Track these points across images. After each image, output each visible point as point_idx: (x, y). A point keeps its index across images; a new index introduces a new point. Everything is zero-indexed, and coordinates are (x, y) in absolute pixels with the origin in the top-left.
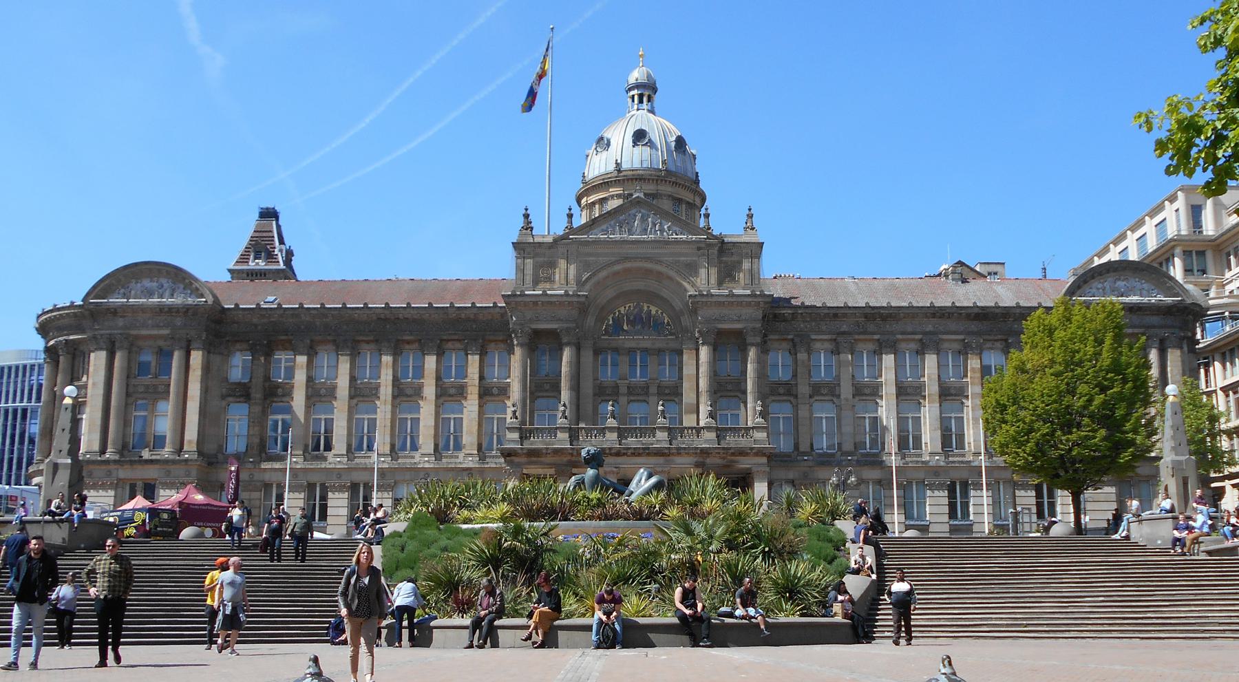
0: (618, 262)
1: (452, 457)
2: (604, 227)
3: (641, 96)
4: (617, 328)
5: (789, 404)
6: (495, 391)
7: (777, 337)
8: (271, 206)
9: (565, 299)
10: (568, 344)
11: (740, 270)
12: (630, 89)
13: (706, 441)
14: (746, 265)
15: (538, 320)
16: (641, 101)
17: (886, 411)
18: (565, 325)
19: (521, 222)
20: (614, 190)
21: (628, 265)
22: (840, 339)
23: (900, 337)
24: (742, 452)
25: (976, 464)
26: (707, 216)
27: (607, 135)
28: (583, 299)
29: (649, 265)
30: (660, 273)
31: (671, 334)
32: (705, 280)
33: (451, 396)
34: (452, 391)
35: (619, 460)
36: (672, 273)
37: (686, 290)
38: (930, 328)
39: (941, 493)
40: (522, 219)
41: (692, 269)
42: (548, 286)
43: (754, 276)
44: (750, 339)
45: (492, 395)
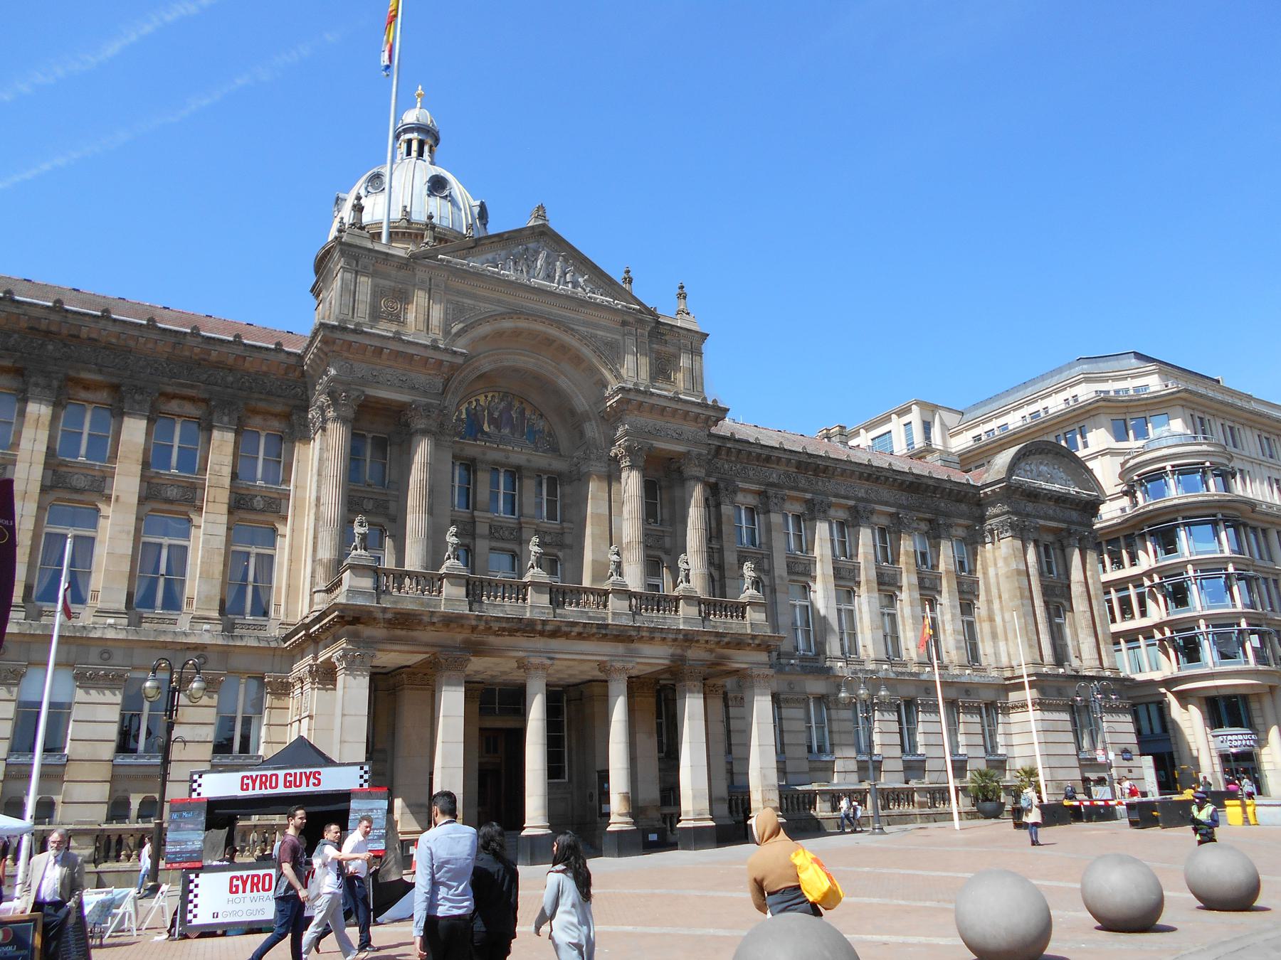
1: (162, 620)
2: (490, 256)
6: (258, 503)
9: (430, 353)
10: (425, 432)
11: (677, 369)
12: (405, 131)
13: (686, 620)
14: (684, 361)
15: (377, 383)
17: (822, 596)
18: (424, 400)
21: (522, 324)
22: (771, 491)
23: (834, 500)
24: (739, 642)
25: (924, 677)
28: (460, 360)
29: (553, 332)
30: (564, 348)
32: (633, 369)
33: (171, 502)
34: (173, 493)
35: (555, 644)
36: (587, 352)
38: (862, 494)
41: (613, 354)
43: (695, 379)
45: (253, 510)
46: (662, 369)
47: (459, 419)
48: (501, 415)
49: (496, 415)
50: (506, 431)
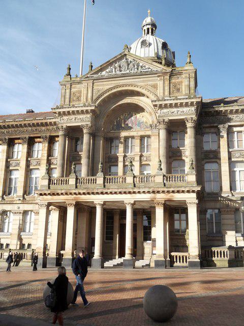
0: (114, 88)
3: (148, 29)
5: (216, 164)
7: (207, 125)
16: (148, 33)
19: (66, 72)
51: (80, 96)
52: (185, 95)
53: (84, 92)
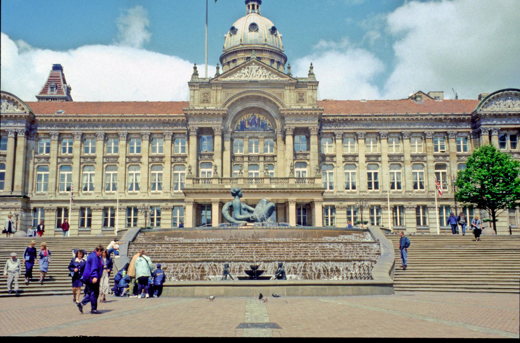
3: (253, 5)
4: (243, 127)
8: (59, 63)
16: (253, 8)
20: (241, 55)
26: (289, 68)
27: (236, 25)
31: (271, 130)
37: (278, 107)
39: (411, 212)
40: (193, 70)
42: (206, 105)
44: (312, 133)
46: (301, 99)
47: (238, 125)
48: (252, 122)
49: (250, 121)
50: (254, 126)
51: (210, 98)
52: (310, 105)
53: (213, 93)
